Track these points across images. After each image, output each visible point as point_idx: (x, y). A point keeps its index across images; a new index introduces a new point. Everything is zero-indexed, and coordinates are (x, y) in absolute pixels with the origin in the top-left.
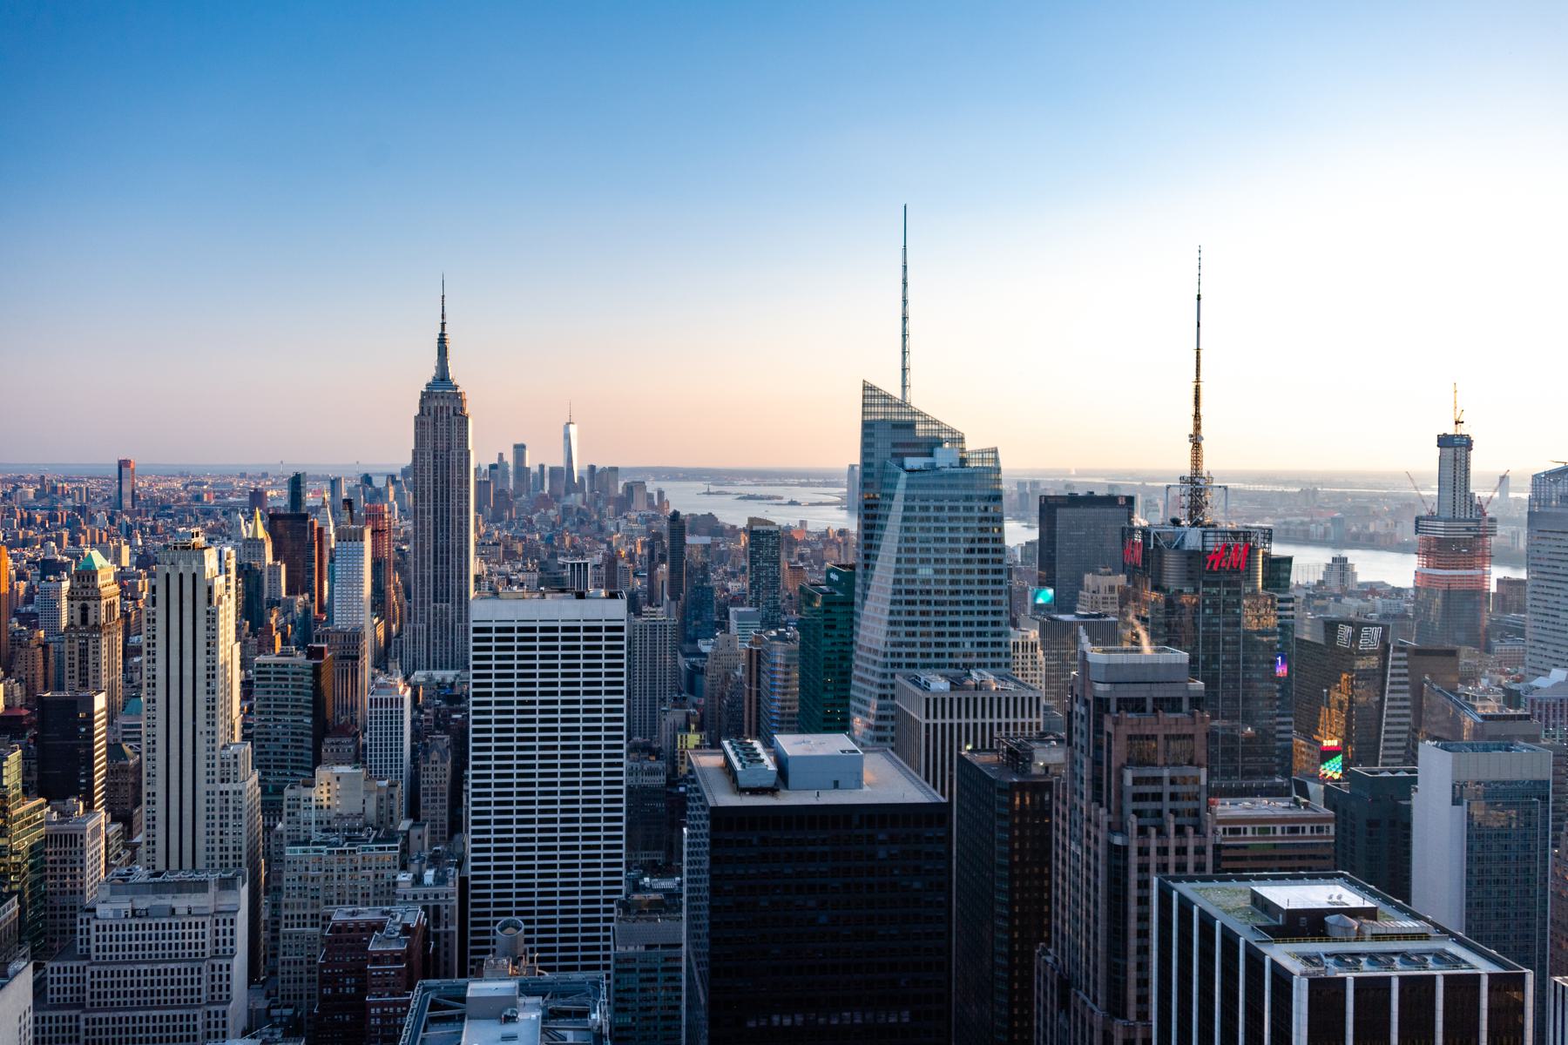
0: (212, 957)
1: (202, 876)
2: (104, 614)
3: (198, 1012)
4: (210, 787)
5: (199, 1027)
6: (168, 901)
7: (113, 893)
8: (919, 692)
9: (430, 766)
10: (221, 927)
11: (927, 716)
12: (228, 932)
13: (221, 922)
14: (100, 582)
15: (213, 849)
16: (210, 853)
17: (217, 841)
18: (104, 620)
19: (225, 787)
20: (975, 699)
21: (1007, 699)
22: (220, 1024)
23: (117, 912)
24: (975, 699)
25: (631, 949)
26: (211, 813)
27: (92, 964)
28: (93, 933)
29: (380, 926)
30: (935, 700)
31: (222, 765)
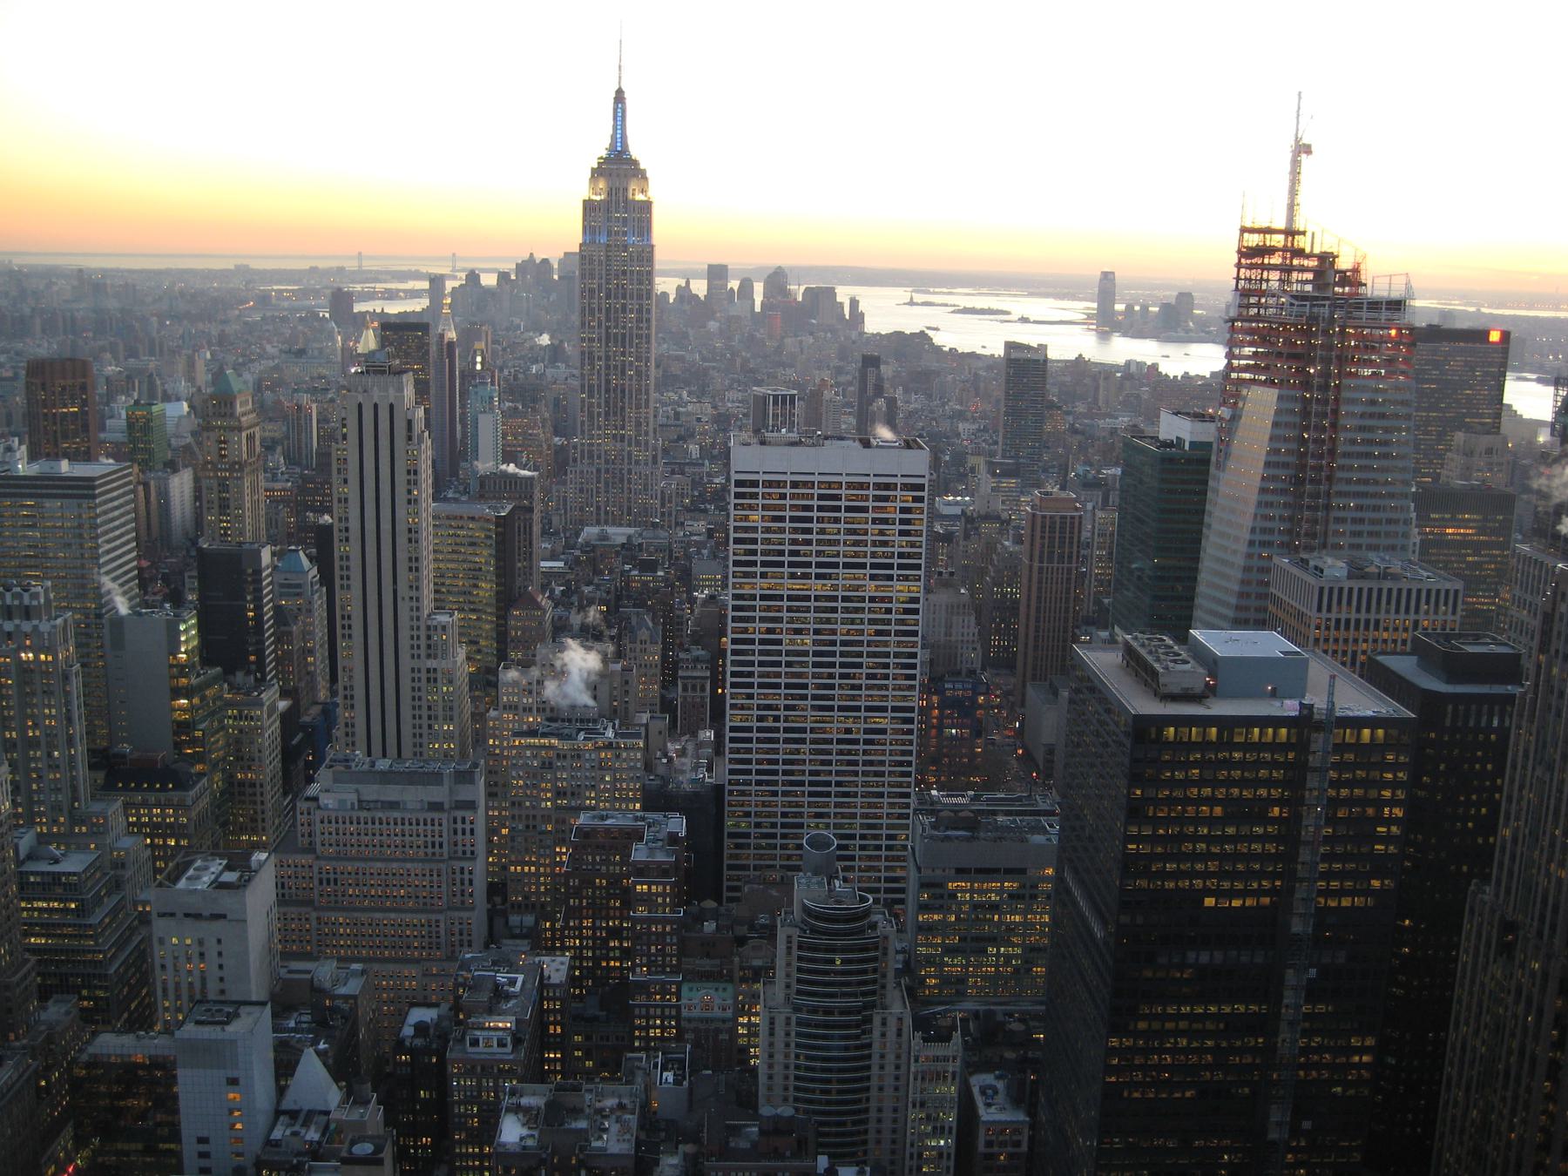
0: (450, 858)
1: (434, 766)
2: (245, 449)
3: (441, 917)
4: (416, 663)
5: (442, 933)
6: (392, 793)
7: (336, 781)
8: (1311, 580)
9: (638, 646)
10: (459, 826)
11: (1319, 609)
12: (468, 831)
13: (459, 821)
14: (239, 409)
15: (421, 735)
16: (418, 740)
17: (425, 726)
18: (245, 456)
19: (431, 663)
20: (1380, 590)
21: (1419, 591)
22: (465, 933)
23: (342, 802)
24: (1380, 590)
25: (939, 872)
26: (417, 694)
27: (318, 858)
28: (318, 824)
29: (636, 835)
30: (1331, 590)
31: (429, 637)
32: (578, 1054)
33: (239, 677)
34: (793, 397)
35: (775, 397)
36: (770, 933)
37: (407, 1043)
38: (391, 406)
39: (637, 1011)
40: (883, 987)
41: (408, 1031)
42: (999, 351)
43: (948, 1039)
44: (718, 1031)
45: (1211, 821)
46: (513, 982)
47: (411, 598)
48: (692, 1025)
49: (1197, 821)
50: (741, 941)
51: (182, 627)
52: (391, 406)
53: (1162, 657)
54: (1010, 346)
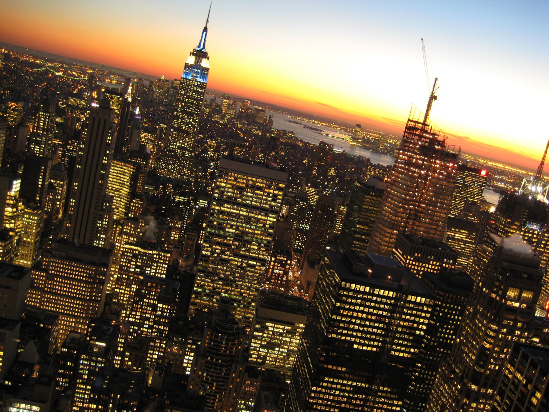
19: (101, 213)
21: (444, 254)
24: (431, 251)
30: (415, 248)
32: (127, 359)
33: (32, 204)
34: (244, 145)
35: (238, 144)
36: (201, 330)
37: (67, 345)
38: (105, 120)
39: (150, 348)
40: (238, 355)
41: (69, 340)
42: (318, 144)
43: (257, 377)
44: (177, 360)
45: (361, 319)
46: (109, 330)
47: (99, 189)
48: (168, 356)
49: (357, 318)
50: (191, 330)
51: (15, 182)
52: (105, 120)
53: (356, 260)
54: (321, 143)
